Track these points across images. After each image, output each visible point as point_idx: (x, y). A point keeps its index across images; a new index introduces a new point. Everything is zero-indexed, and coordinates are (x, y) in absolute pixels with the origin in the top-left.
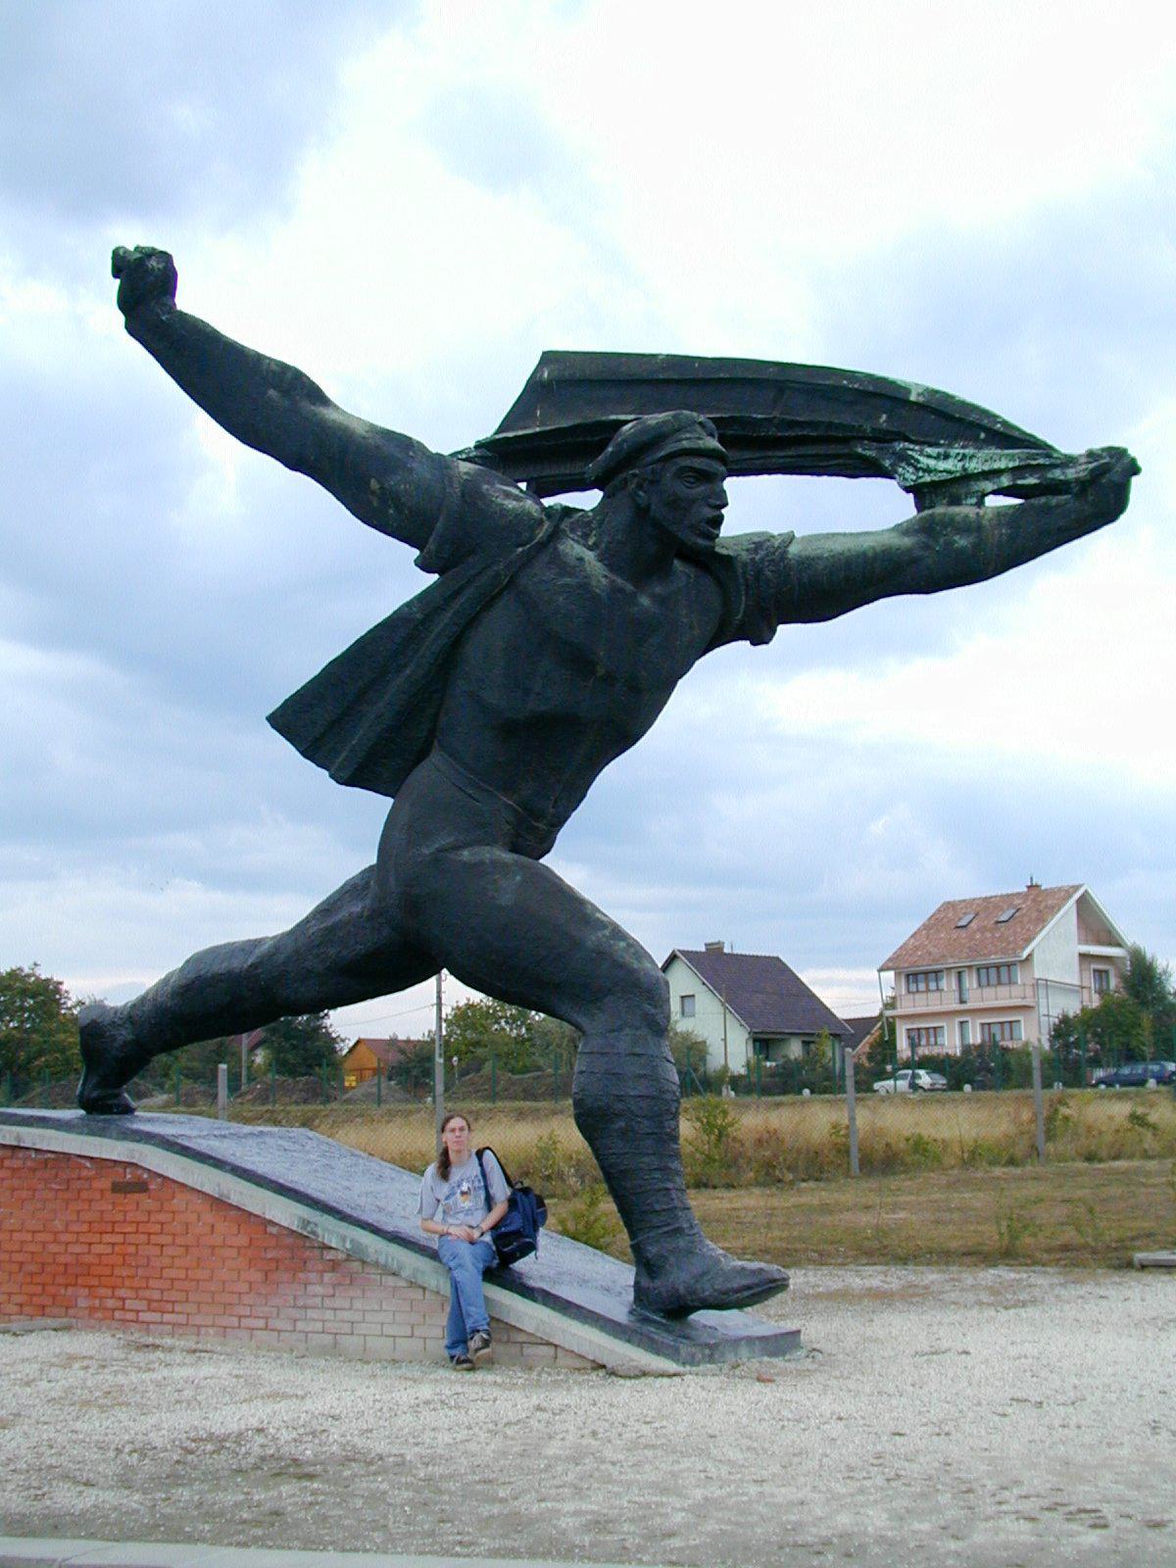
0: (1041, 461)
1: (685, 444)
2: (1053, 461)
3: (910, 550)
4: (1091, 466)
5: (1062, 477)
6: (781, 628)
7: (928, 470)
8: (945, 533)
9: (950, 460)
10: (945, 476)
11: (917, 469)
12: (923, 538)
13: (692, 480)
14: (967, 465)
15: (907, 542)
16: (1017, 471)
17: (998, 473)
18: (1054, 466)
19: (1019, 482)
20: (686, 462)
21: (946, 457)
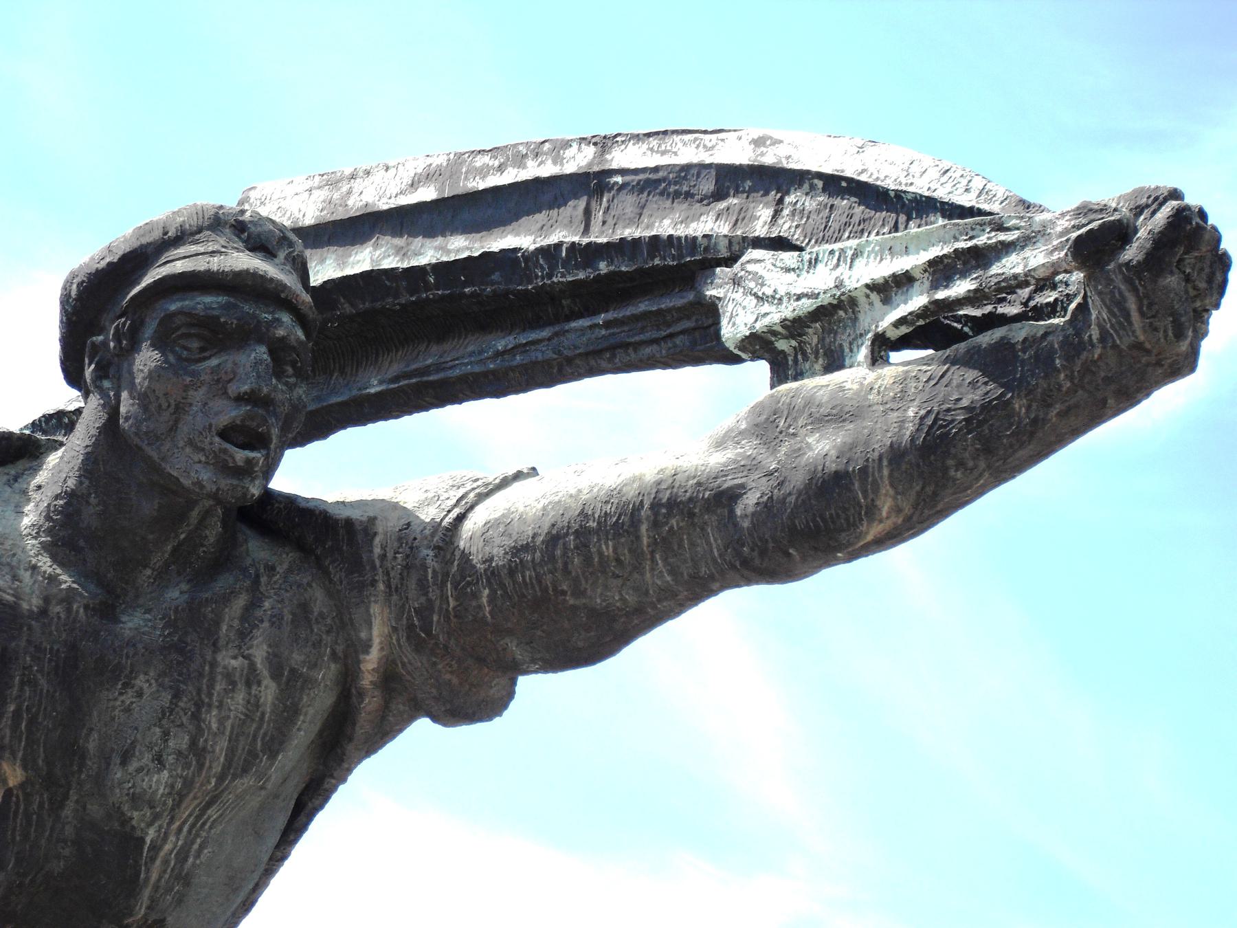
0: (982, 240)
1: (179, 267)
2: (1002, 237)
3: (722, 473)
4: (1074, 235)
5: (1019, 270)
6: (522, 680)
7: (775, 299)
8: (791, 431)
9: (820, 266)
10: (807, 305)
11: (760, 299)
12: (749, 448)
13: (195, 344)
14: (845, 277)
15: (718, 459)
16: (942, 270)
17: (903, 281)
18: (1005, 248)
19: (941, 295)
20: (173, 307)
21: (813, 263)
